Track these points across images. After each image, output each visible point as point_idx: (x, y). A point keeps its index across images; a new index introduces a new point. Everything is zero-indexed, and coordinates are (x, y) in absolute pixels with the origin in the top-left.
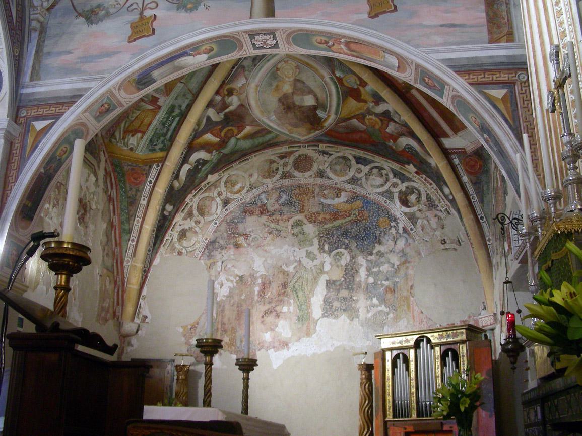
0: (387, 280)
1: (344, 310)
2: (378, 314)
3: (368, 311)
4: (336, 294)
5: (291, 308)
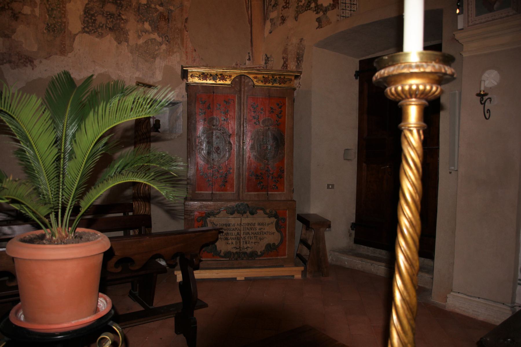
0: (161, 5)
1: (110, 28)
2: (150, 43)
3: (139, 37)
4: (101, 6)
5: (37, 11)
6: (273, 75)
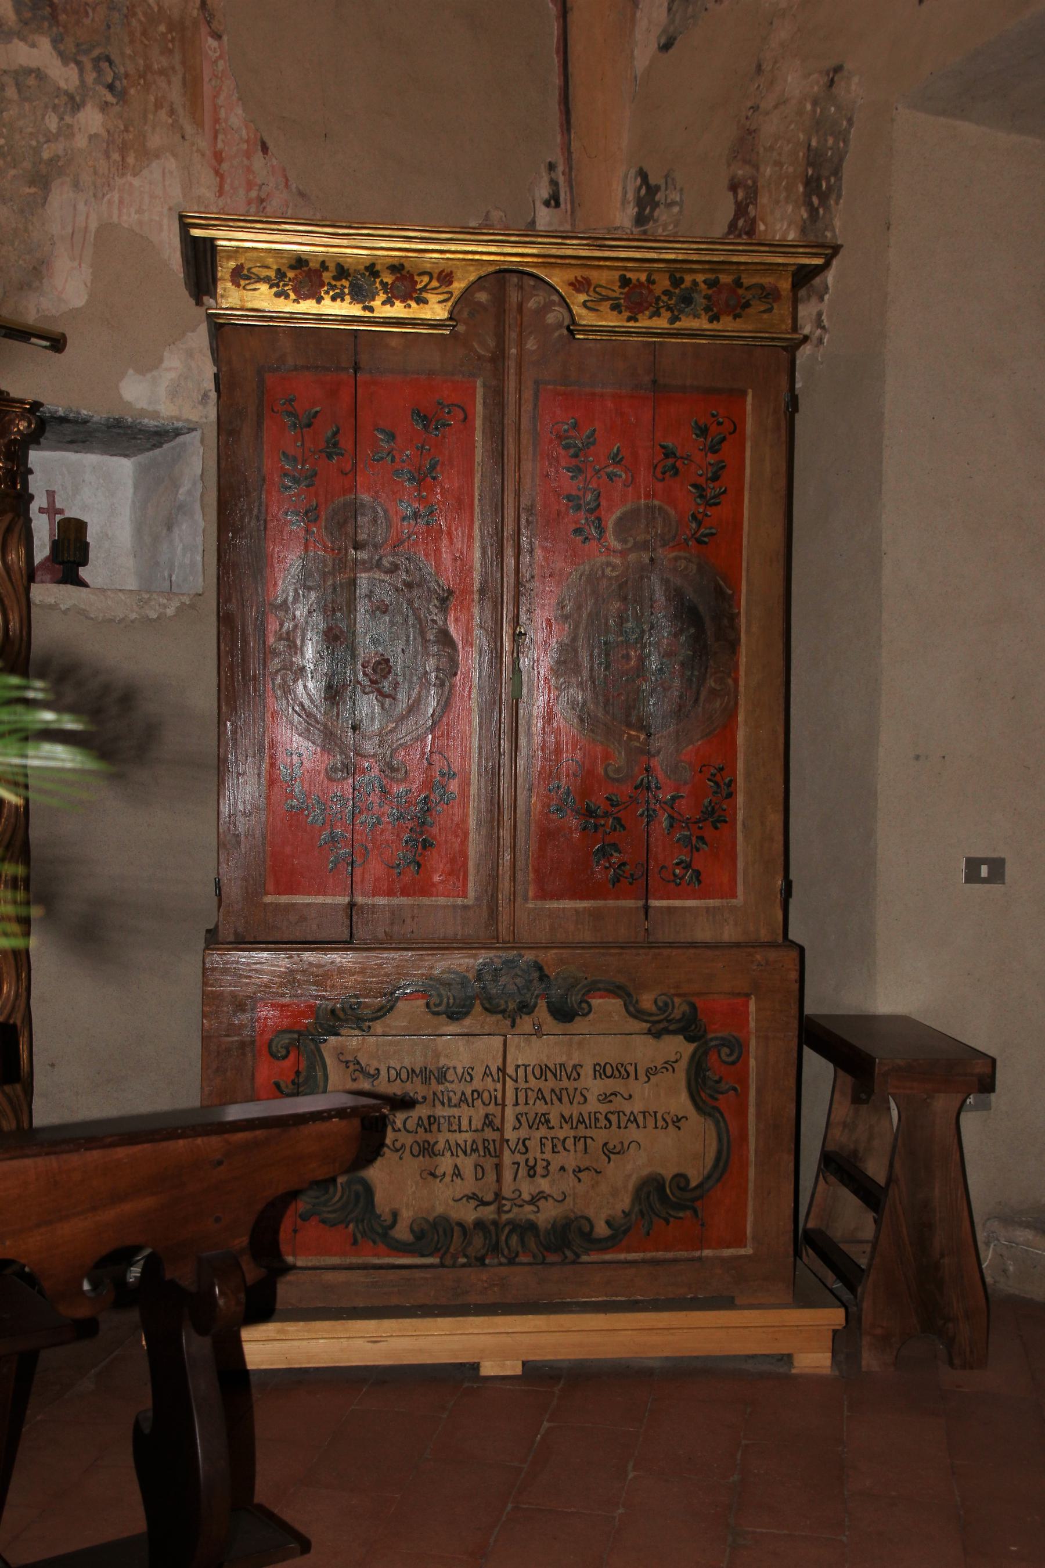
6: (676, 272)
